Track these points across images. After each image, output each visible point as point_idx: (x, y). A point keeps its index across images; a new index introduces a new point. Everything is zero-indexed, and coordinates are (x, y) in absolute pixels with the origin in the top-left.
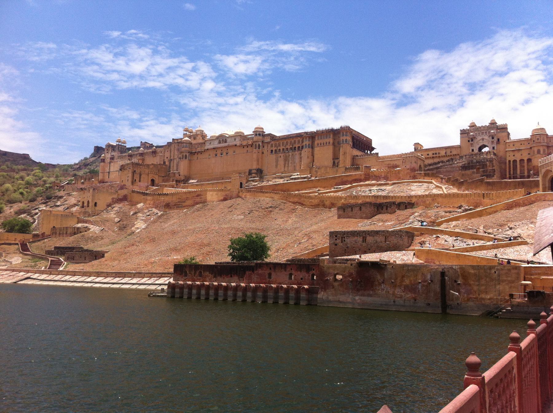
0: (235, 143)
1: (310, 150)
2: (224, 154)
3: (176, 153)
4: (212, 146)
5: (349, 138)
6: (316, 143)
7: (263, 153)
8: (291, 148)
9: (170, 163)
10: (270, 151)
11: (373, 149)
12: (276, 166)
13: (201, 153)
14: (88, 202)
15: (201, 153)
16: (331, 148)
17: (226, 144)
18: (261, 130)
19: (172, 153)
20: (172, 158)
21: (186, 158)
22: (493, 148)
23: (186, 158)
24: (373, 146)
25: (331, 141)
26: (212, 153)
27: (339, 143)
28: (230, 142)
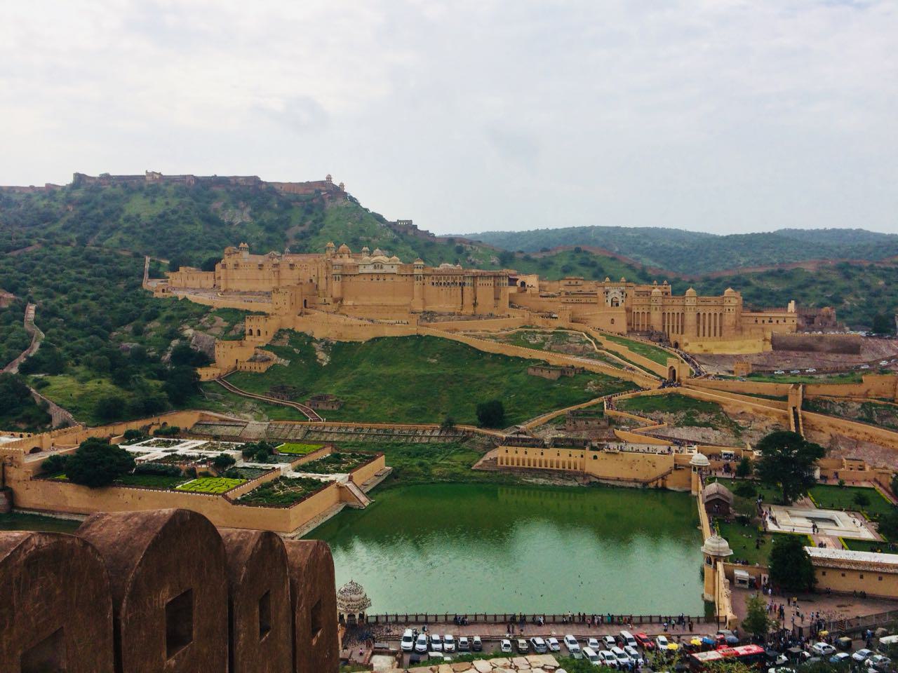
0: (392, 271)
2: (381, 280)
4: (365, 271)
5: (507, 282)
6: (478, 283)
7: (424, 284)
14: (259, 331)
15: (355, 275)
16: (493, 289)
17: (382, 271)
21: (339, 280)
23: (339, 280)
25: (492, 284)
26: (368, 278)
27: (498, 284)
28: (387, 269)
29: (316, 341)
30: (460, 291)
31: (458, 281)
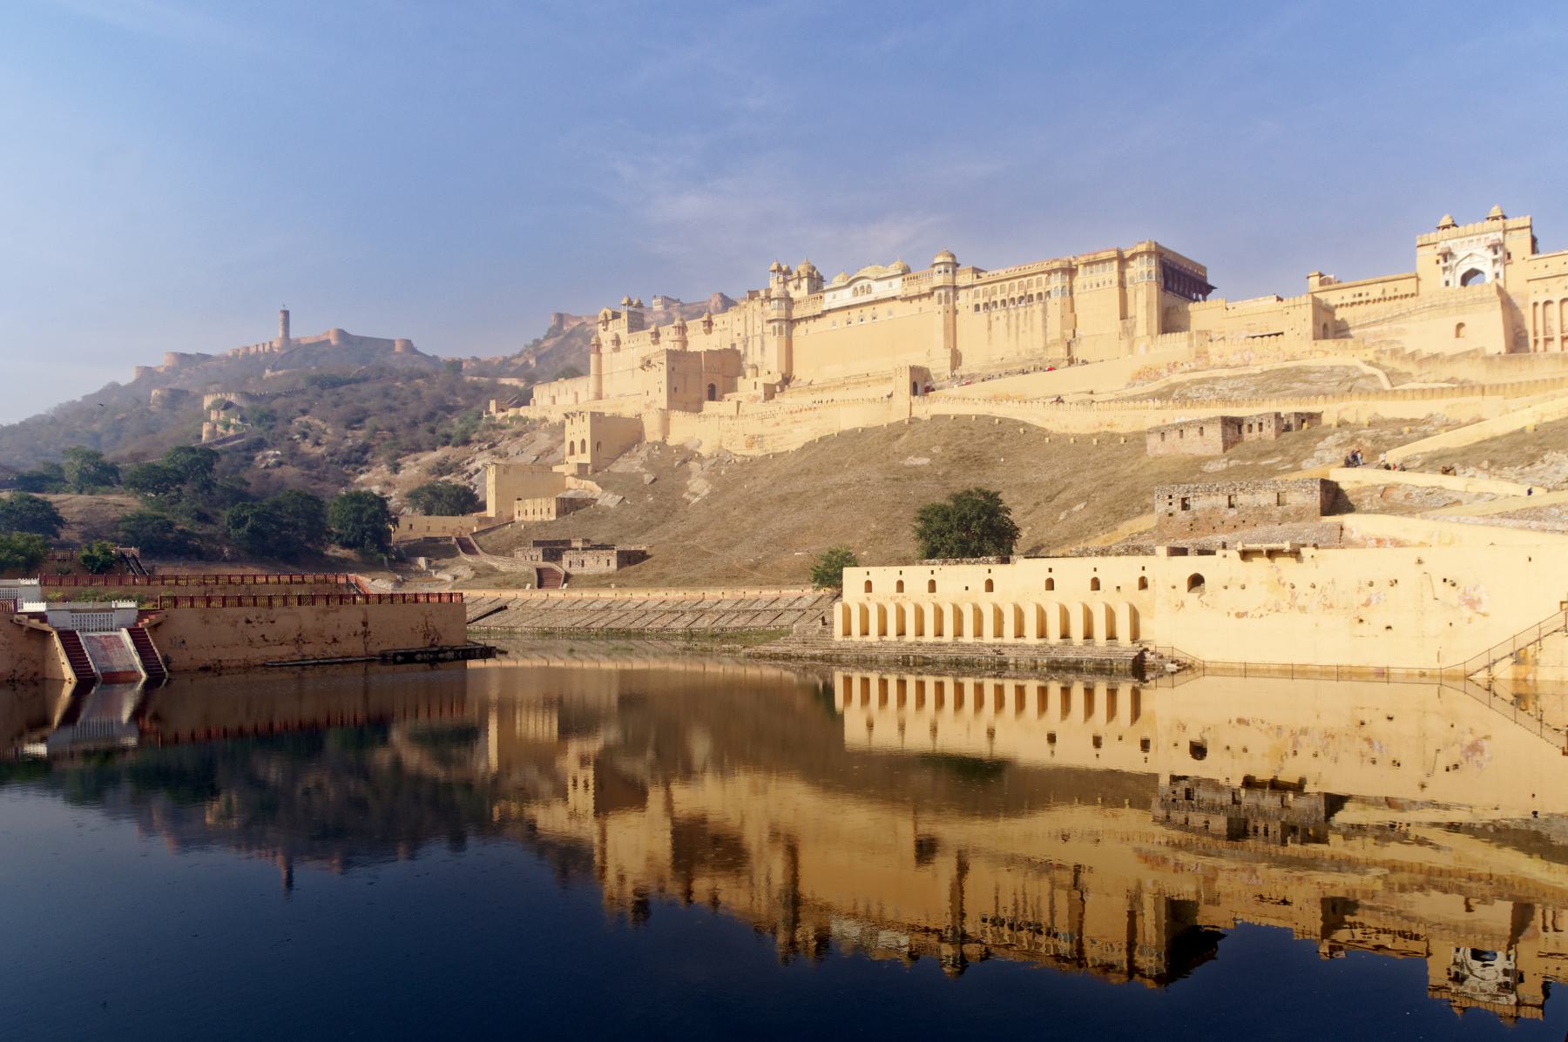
2: (868, 320)
3: (758, 323)
7: (956, 312)
8: (1022, 298)
10: (972, 308)
11: (1210, 289)
13: (815, 317)
16: (1116, 291)
17: (870, 298)
19: (750, 323)
20: (750, 334)
22: (1497, 275)
23: (781, 333)
24: (1210, 282)
25: (1115, 278)
28: (880, 290)
29: (700, 458)
31: (1034, 291)
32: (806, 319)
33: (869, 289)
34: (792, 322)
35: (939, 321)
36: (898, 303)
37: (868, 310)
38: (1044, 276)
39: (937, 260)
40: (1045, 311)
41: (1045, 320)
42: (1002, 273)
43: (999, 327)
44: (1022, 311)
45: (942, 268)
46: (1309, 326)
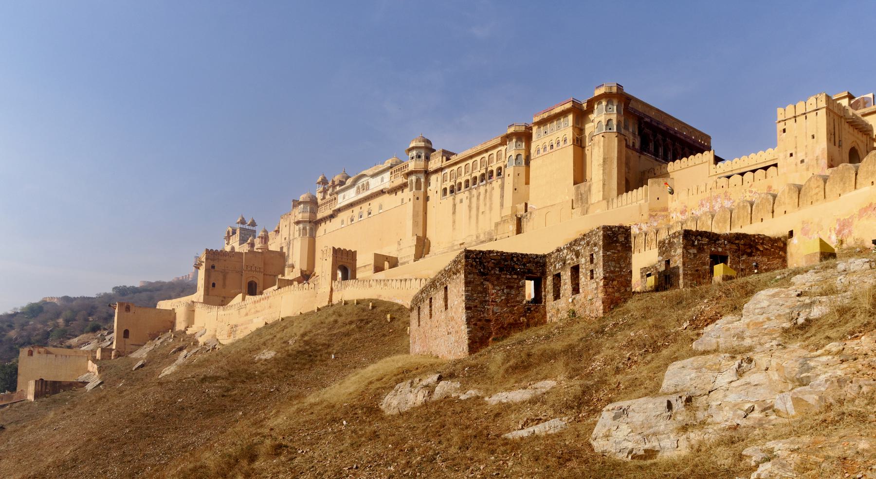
1: (523, 168)
2: (365, 215)
9: (289, 249)
12: (454, 222)
16: (569, 151)
18: (422, 144)
19: (292, 228)
23: (305, 234)
30: (497, 192)
32: (324, 219)
33: (366, 187)
34: (315, 223)
35: (409, 207)
36: (387, 195)
37: (365, 206)
38: (503, 148)
39: (412, 145)
40: (502, 187)
41: (502, 196)
42: (469, 152)
43: (462, 209)
44: (482, 189)
45: (414, 153)
46: (822, 144)
